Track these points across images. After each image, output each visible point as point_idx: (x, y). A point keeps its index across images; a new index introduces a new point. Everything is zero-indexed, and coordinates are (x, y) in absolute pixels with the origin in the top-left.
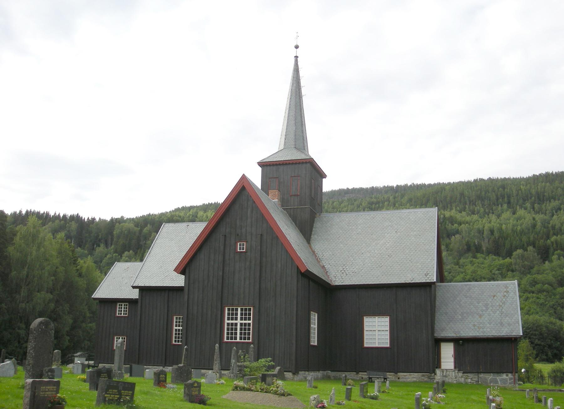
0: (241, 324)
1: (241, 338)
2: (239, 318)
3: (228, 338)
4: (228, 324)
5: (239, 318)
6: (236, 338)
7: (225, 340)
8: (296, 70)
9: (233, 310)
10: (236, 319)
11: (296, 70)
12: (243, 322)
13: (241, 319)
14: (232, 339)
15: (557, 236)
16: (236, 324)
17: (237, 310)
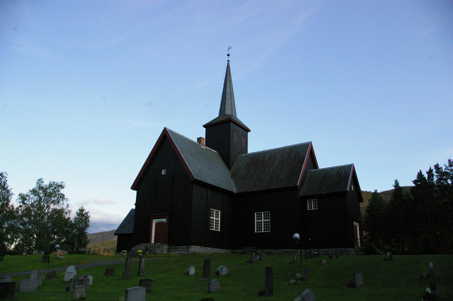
0: (264, 222)
1: (264, 230)
2: (263, 219)
3: (257, 231)
4: (257, 222)
5: (263, 219)
6: (261, 230)
7: (256, 232)
8: (228, 67)
9: (259, 214)
10: (261, 219)
11: (228, 67)
12: (265, 220)
13: (264, 219)
14: (259, 231)
15: (437, 172)
16: (261, 222)
17: (261, 214)
